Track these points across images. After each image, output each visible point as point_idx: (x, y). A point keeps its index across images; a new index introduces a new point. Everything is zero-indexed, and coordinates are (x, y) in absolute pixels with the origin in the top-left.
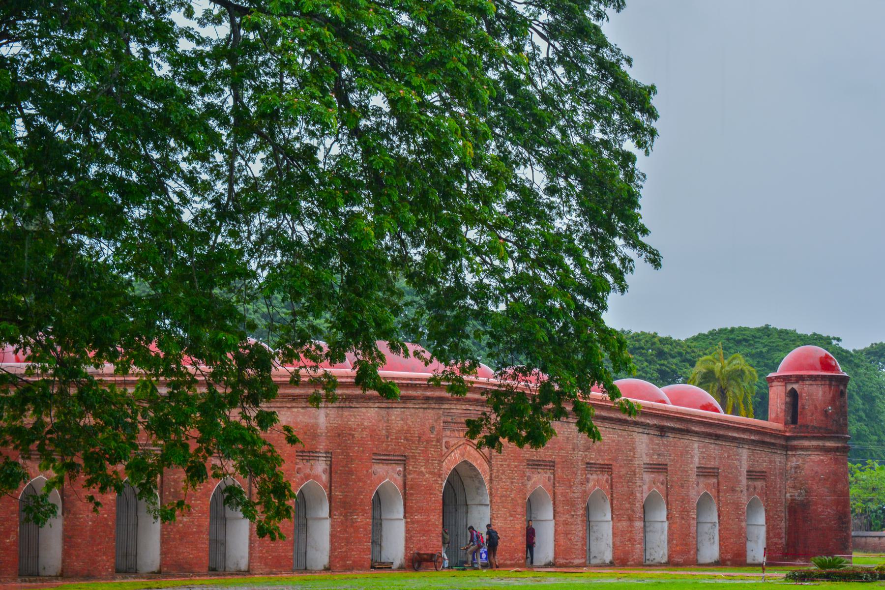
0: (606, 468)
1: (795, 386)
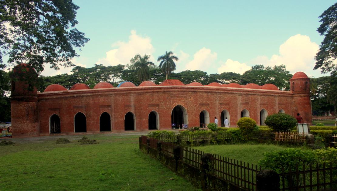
0: (228, 104)
1: (294, 82)
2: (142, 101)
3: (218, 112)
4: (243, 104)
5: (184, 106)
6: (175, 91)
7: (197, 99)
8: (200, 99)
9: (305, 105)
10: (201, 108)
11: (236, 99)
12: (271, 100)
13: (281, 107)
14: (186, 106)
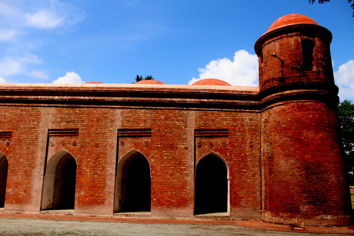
9: (305, 133)
11: (38, 118)
12: (166, 119)
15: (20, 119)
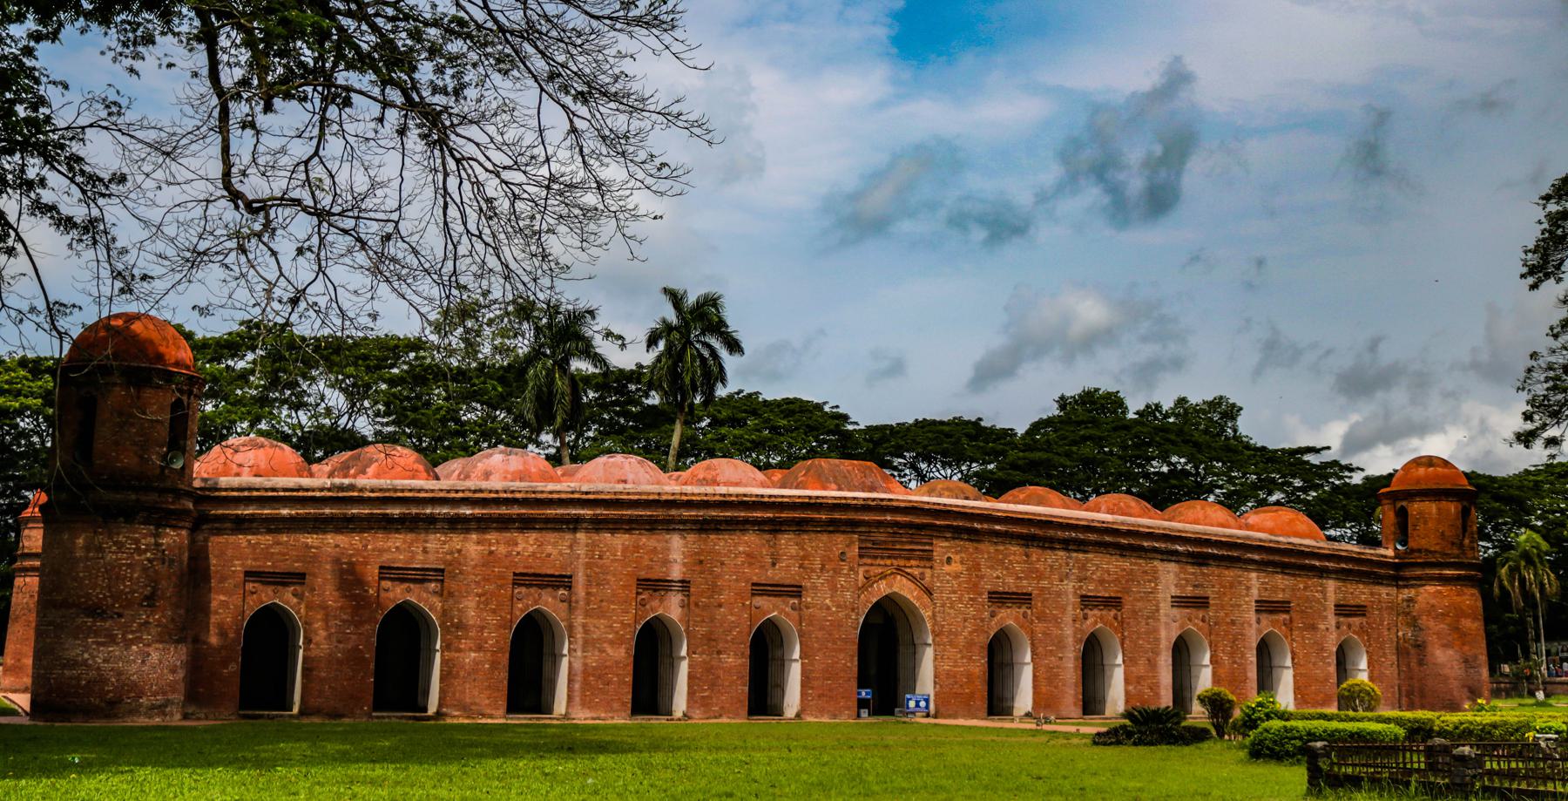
0: (1113, 603)
1: (1404, 503)
2: (722, 564)
3: (1070, 640)
4: (1180, 602)
5: (918, 598)
6: (880, 524)
7: (977, 567)
8: (992, 567)
10: (993, 615)
12: (1305, 588)
13: (1349, 626)
14: (926, 598)
15: (1131, 577)
